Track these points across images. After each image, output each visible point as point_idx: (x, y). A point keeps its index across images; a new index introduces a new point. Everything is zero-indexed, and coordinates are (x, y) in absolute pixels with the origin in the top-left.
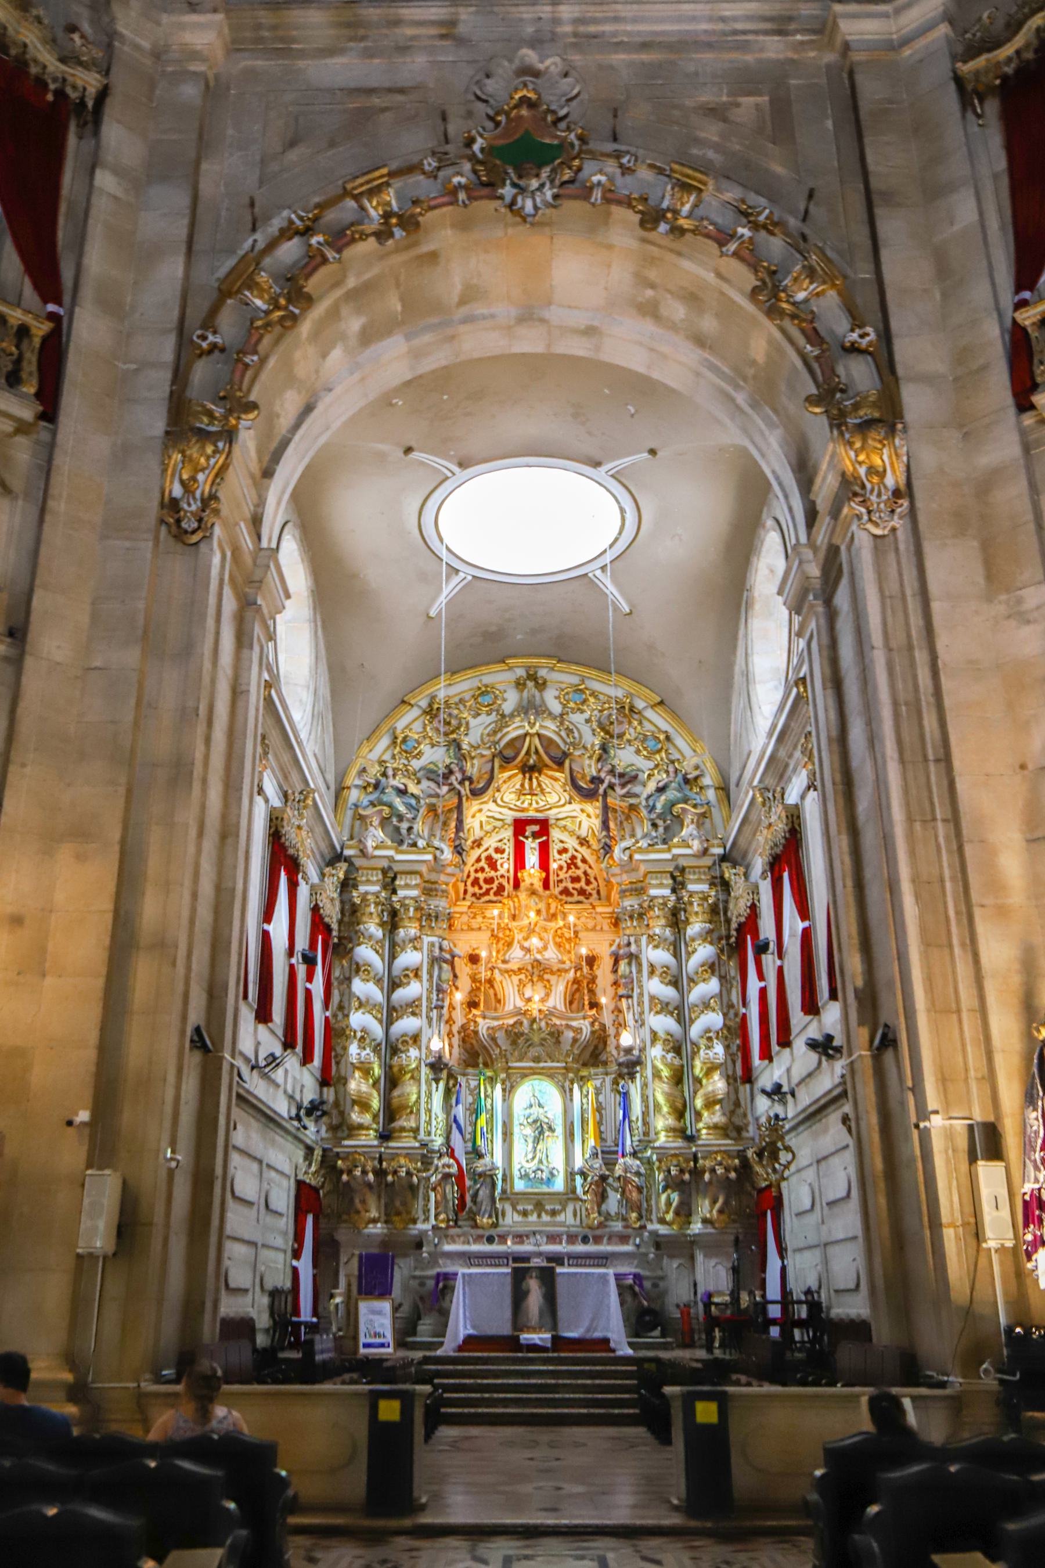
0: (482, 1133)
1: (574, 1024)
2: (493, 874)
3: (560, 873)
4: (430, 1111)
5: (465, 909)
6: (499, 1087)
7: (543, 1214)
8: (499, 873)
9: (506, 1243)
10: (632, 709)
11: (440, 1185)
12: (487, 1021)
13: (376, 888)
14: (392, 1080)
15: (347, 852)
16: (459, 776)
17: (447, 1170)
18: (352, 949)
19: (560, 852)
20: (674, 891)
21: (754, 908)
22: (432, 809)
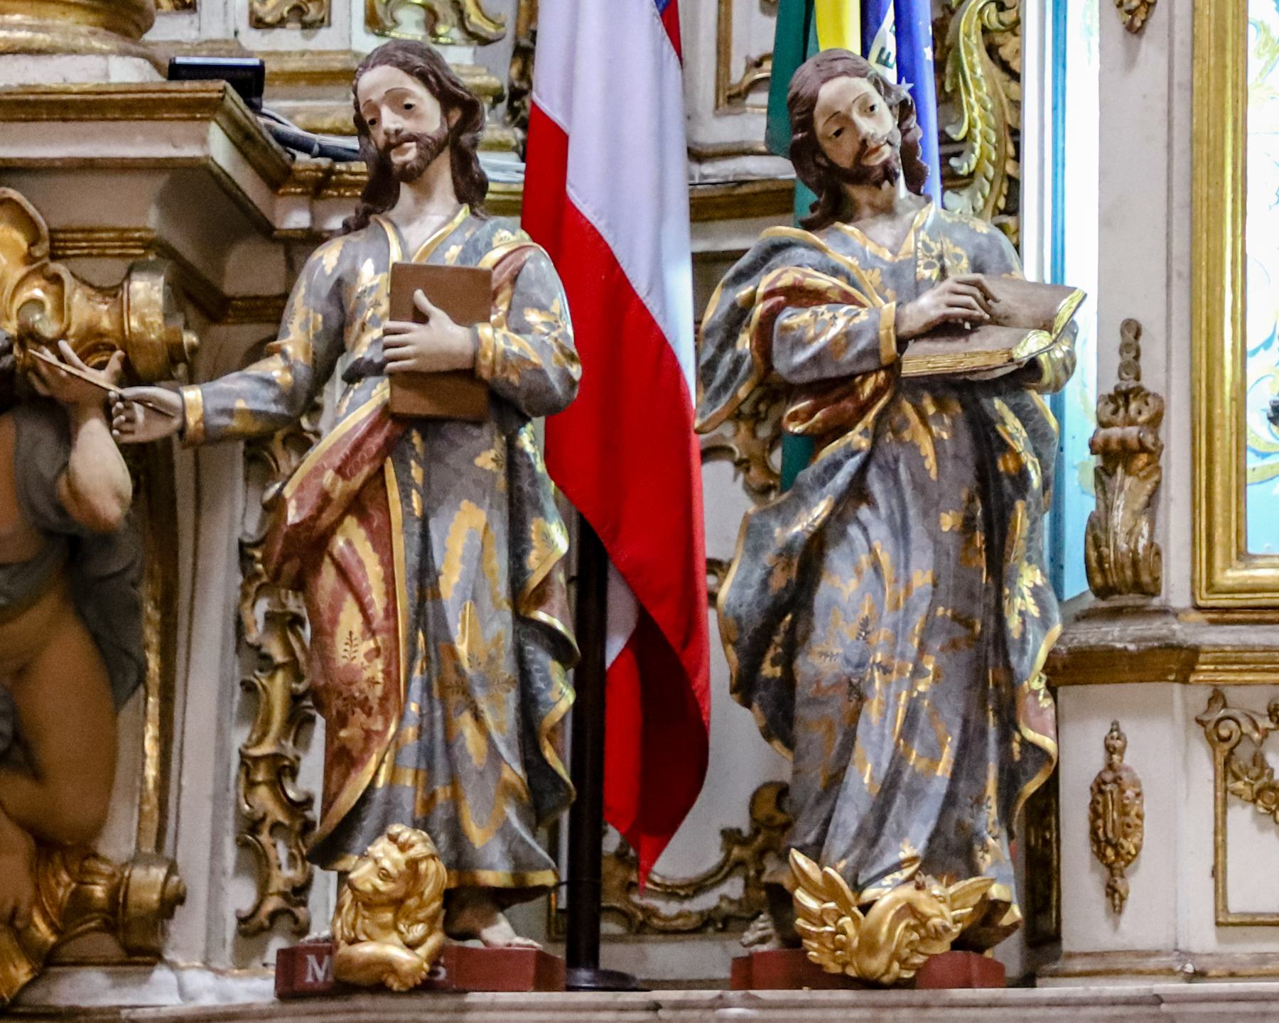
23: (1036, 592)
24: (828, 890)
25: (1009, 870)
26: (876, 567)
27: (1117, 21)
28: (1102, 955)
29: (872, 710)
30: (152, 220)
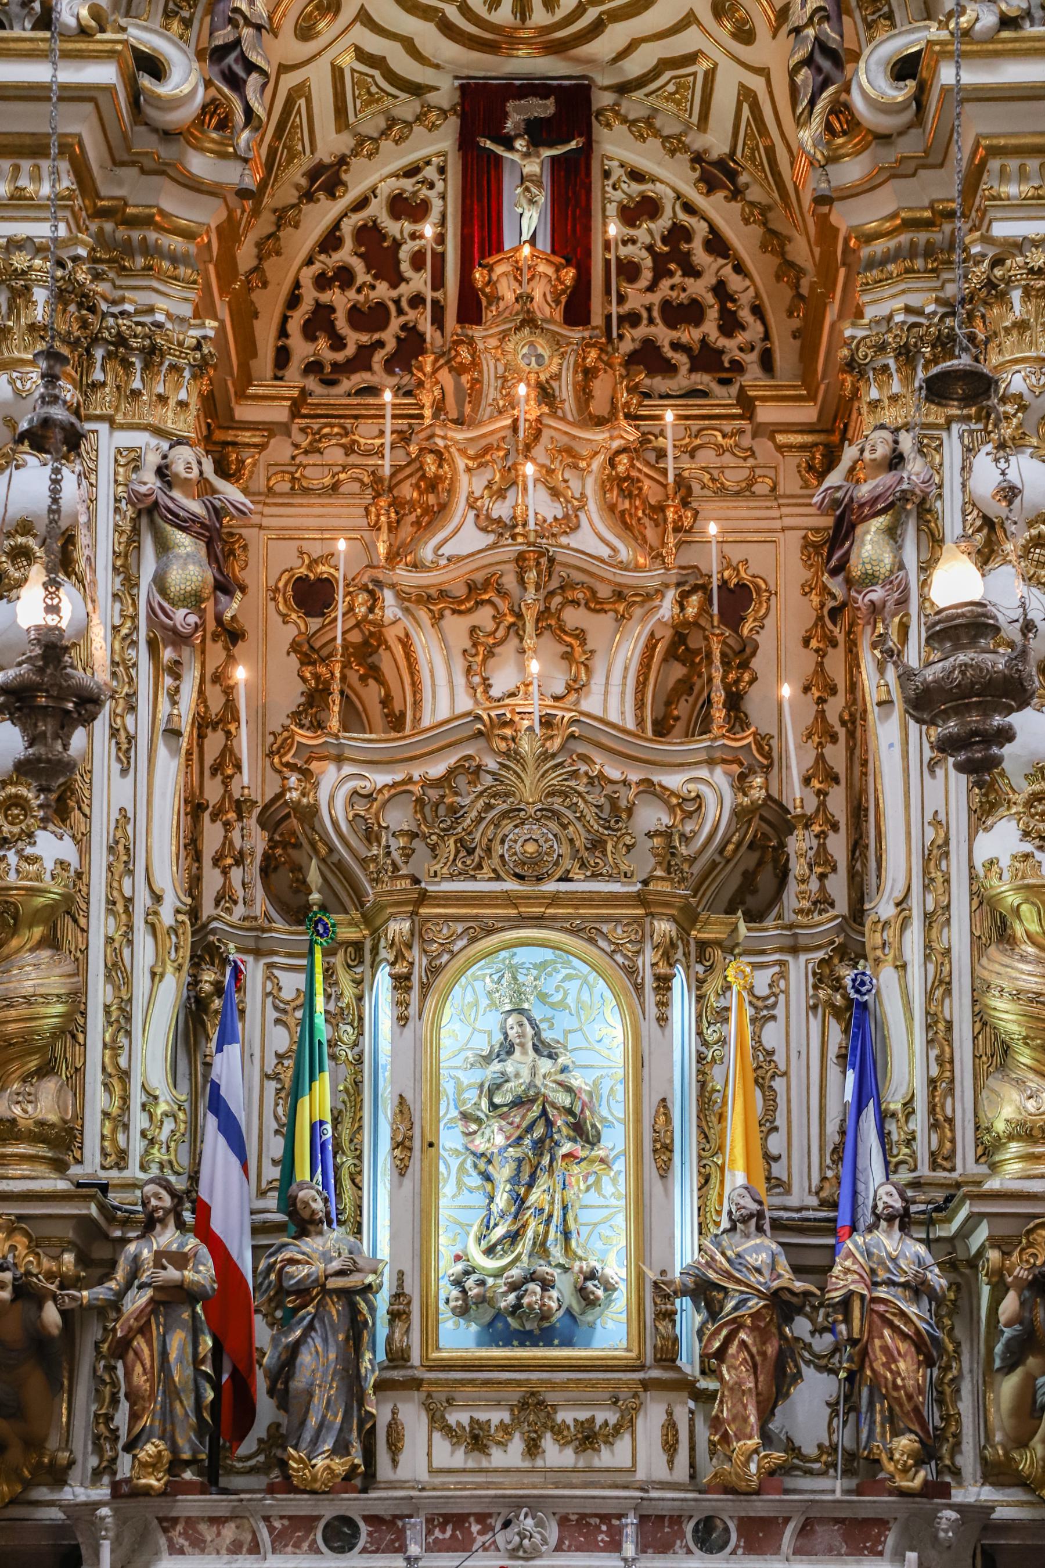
0: (317, 1147)
1: (674, 781)
2: (382, 291)
3: (629, 290)
4: (125, 1076)
5: (279, 413)
6: (383, 979)
7: (548, 1442)
8: (405, 290)
9: (402, 1549)
11: (144, 1330)
12: (348, 769)
17: (172, 1274)
19: (630, 215)
23: (370, 1360)
24: (300, 1461)
25: (360, 1454)
26: (317, 1352)
27: (396, 1172)
28: (391, 1482)
29: (316, 1400)
30: (71, 1234)
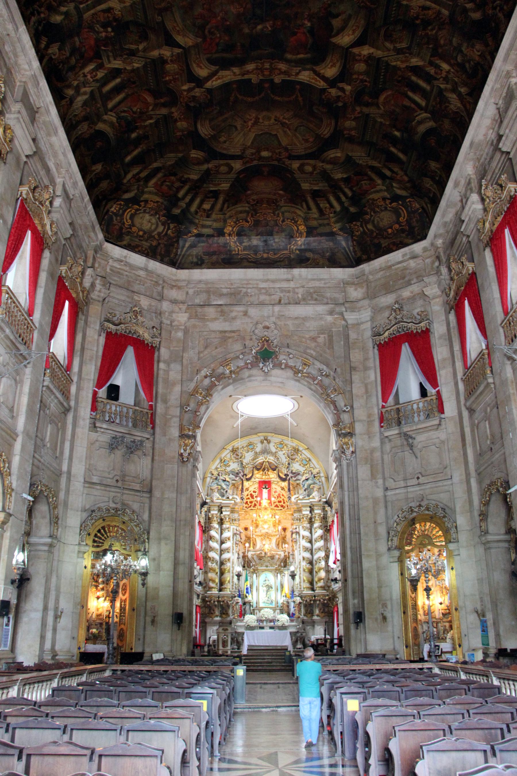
10: (298, 450)
13: (216, 512)
14: (222, 573)
15: (207, 501)
16: (242, 474)
18: (209, 531)
20: (311, 512)
21: (333, 521)
22: (234, 485)
